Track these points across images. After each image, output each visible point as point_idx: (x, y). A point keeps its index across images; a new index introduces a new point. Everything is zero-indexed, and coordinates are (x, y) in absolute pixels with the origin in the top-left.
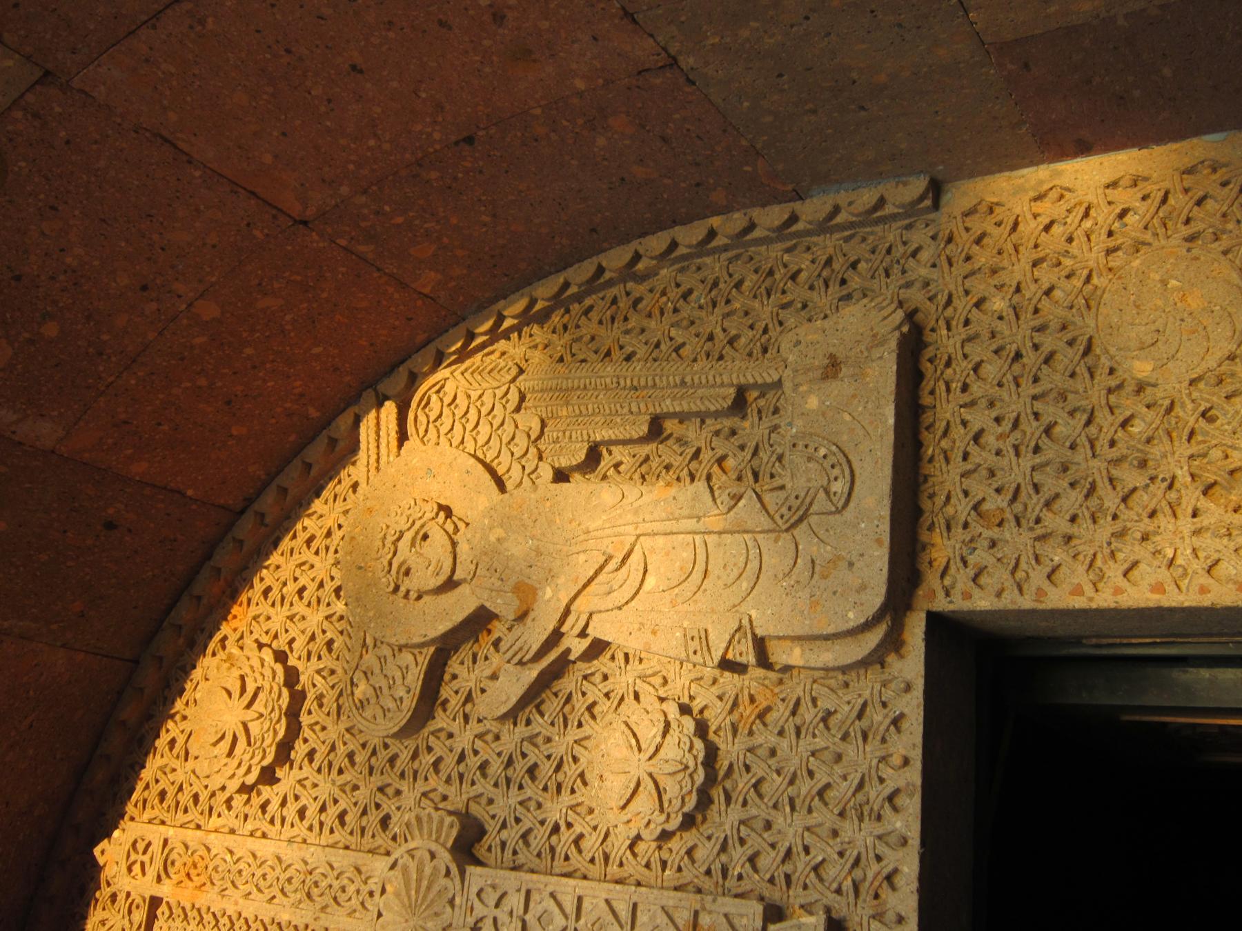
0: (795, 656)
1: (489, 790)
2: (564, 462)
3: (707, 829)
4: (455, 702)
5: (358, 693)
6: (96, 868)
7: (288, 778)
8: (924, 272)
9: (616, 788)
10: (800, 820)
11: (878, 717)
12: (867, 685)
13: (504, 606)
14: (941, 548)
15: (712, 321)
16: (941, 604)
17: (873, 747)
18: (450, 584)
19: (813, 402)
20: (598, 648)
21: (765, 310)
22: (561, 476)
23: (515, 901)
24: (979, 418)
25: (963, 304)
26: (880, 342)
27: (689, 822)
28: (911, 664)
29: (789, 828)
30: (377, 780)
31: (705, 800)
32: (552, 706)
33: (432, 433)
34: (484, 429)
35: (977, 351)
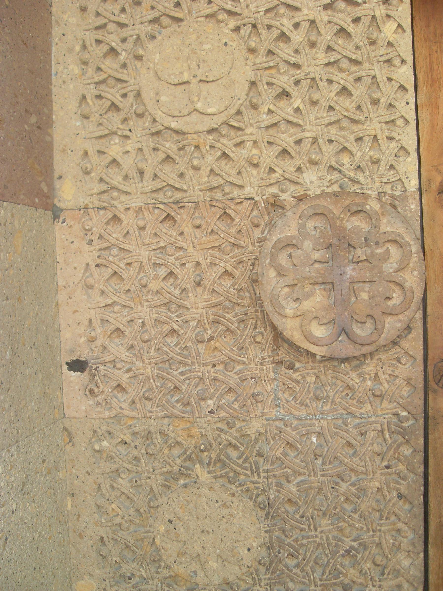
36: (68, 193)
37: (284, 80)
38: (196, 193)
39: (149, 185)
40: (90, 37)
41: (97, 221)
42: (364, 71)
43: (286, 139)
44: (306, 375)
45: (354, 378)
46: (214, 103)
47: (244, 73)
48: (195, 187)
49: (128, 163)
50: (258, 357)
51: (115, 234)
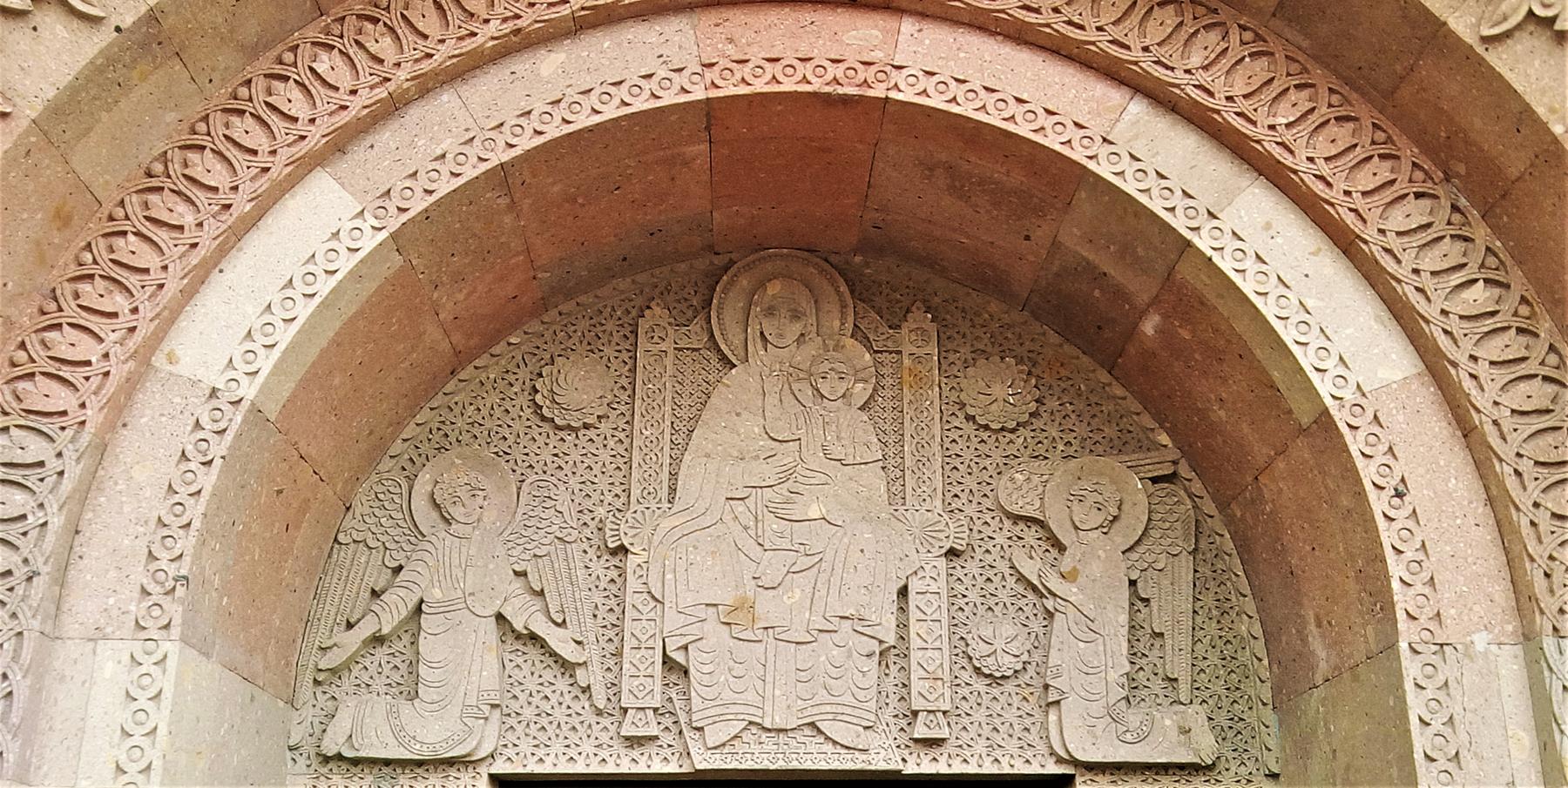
0: (1053, 717)
2: (1139, 585)
3: (974, 676)
4: (1018, 528)
5: (1018, 476)
7: (969, 428)
8: (1233, 769)
9: (987, 632)
10: (983, 720)
12: (1042, 748)
13: (1067, 563)
15: (1214, 658)
16: (1078, 780)
17: (1016, 752)
19: (1168, 722)
20: (1050, 615)
22: (1133, 583)
23: (934, 588)
26: (1197, 752)
27: (977, 670)
28: (1053, 769)
29: (980, 715)
30: (975, 487)
31: (987, 676)
32: (1021, 590)
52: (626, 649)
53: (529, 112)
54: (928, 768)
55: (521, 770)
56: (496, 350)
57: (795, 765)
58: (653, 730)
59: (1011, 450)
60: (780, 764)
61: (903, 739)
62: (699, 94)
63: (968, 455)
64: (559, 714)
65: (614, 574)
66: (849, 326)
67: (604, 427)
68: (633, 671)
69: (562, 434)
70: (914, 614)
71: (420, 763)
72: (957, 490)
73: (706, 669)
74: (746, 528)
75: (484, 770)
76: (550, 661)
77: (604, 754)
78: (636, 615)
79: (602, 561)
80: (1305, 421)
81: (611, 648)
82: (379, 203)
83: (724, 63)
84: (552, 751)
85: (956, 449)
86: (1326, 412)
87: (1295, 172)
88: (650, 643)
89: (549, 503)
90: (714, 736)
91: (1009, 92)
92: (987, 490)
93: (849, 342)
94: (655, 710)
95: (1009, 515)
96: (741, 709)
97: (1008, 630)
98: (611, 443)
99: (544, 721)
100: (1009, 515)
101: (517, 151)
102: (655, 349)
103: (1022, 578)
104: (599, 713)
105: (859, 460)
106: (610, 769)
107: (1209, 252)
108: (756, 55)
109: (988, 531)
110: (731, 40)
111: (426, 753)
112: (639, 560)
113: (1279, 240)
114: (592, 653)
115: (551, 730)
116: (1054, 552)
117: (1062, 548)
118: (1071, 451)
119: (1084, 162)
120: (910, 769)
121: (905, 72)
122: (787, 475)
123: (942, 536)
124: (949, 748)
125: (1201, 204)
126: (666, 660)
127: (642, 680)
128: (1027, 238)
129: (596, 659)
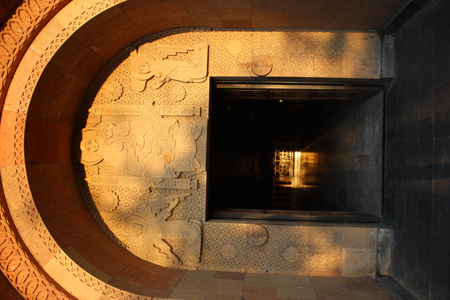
1: (155, 98)
5: (135, 86)
6: (89, 113)
9: (175, 96)
11: (204, 87)
13: (157, 75)
14: (211, 70)
16: (211, 76)
17: (204, 90)
18: (149, 72)
19: (198, 53)
21: (190, 40)
23: (163, 109)
24: (215, 56)
25: (214, 43)
28: (208, 82)
32: (163, 87)
33: (143, 52)
34: (151, 52)
35: (215, 48)
36: (243, 271)
37: (231, 240)
38: (245, 253)
39: (243, 259)
40: (222, 266)
41: (247, 266)
42: (230, 229)
43: (239, 240)
44: (270, 240)
45: (271, 234)
46: (233, 249)
47: (229, 245)
48: (244, 253)
49: (240, 261)
50: (268, 246)
51: (249, 264)
52: (176, 188)
53: (28, 212)
54: (207, 112)
55: (205, 214)
56: (98, 222)
57: (205, 146)
58: (196, 181)
59: (128, 87)
60: (205, 149)
61: (200, 118)
62: (24, 166)
63: (129, 99)
64: (191, 204)
65: (156, 191)
66: (93, 129)
67: (118, 194)
68: (181, 186)
69: (120, 204)
70: (169, 114)
71: (202, 239)
72: (138, 102)
73: (181, 167)
74: (145, 157)
75: (204, 223)
76: (178, 207)
77: (201, 194)
78: (167, 185)
79: (153, 194)
80: (121, 11)
81: (175, 192)
82: (53, 252)
83: (15, 159)
84: (200, 206)
85: (127, 102)
86: (118, 5)
87: (53, 7)
88: (174, 182)
89: (138, 207)
90: (198, 166)
91: (26, 81)
92: (138, 95)
93: (98, 129)
94: (191, 180)
95: (145, 89)
96: (191, 159)
97: (174, 91)
98: (123, 192)
99: (193, 208)
100: (145, 89)
101: (39, 215)
102: (98, 180)
103: (161, 86)
104: (191, 194)
105: (129, 127)
106: (205, 192)
107: (74, 31)
108: (14, 150)
109: (149, 95)
110: (9, 157)
111: (200, 237)
112: (153, 185)
113: (72, 13)
114: (176, 197)
115: (195, 207)
116: (154, 78)
117: (154, 76)
118: (129, 72)
119: (47, 62)
120: (207, 117)
121: (20, 109)
122: (132, 146)
123: (149, 106)
124: (202, 108)
125: (61, 32)
126: (179, 177)
127: (183, 184)
128: (70, 80)
129: (178, 195)
